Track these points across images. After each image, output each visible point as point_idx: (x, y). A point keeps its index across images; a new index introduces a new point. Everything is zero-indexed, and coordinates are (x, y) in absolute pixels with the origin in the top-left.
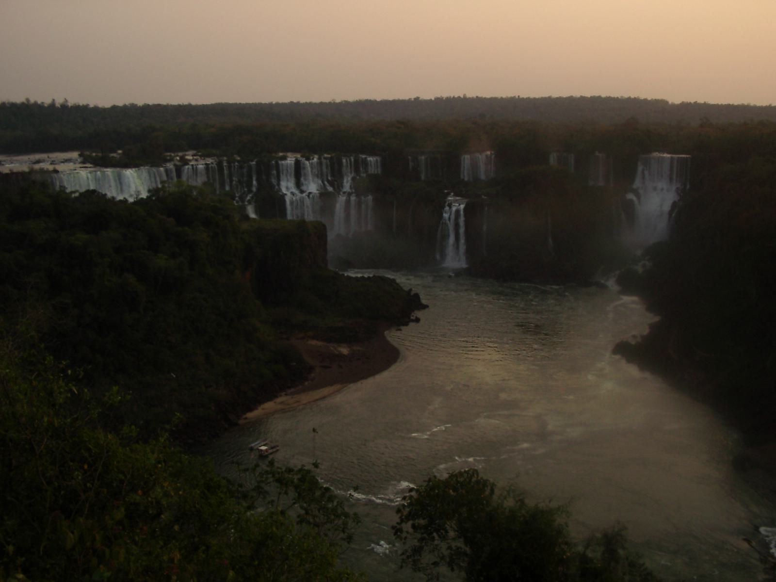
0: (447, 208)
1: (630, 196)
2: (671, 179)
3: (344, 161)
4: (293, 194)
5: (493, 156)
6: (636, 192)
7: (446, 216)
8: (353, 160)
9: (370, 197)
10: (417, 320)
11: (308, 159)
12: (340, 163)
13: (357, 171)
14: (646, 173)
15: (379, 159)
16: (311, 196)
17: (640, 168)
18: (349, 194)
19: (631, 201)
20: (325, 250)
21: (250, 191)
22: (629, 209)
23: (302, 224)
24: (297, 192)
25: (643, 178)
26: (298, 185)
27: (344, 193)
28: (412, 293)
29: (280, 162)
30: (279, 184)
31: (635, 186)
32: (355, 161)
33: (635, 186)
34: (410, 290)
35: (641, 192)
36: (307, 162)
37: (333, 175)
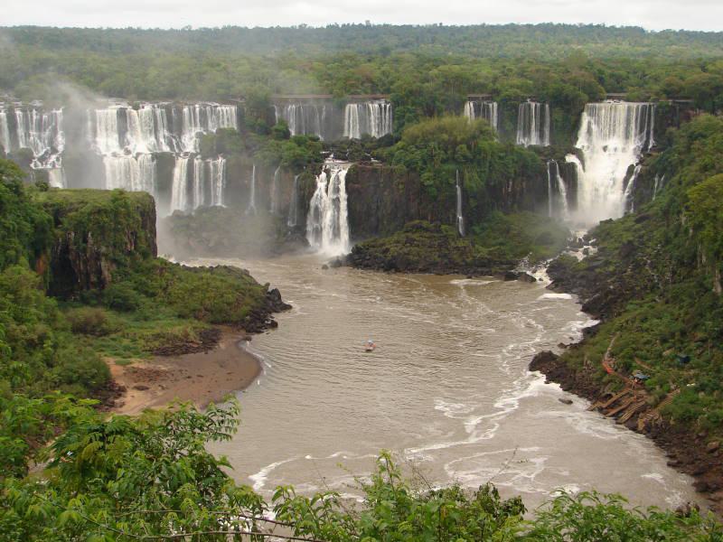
0: (323, 175)
1: (571, 159)
2: (627, 136)
3: (186, 110)
4: (115, 155)
5: (388, 106)
6: (579, 153)
7: (321, 185)
8: (197, 109)
9: (221, 161)
10: (274, 325)
11: (136, 108)
12: (180, 112)
13: (204, 123)
14: (594, 127)
15: (234, 108)
16: (139, 159)
17: (585, 118)
18: (193, 156)
19: (573, 165)
20: (154, 232)
21: (54, 151)
22: (570, 175)
23: (119, 196)
24: (122, 152)
25: (589, 131)
26: (123, 142)
27: (186, 154)
28: (270, 290)
29: (98, 112)
30: (95, 142)
31: (578, 146)
32: (203, 114)
33: (578, 146)
34: (268, 285)
35: (586, 153)
36: (135, 112)
37: (170, 130)
